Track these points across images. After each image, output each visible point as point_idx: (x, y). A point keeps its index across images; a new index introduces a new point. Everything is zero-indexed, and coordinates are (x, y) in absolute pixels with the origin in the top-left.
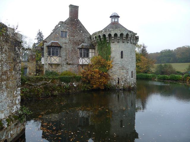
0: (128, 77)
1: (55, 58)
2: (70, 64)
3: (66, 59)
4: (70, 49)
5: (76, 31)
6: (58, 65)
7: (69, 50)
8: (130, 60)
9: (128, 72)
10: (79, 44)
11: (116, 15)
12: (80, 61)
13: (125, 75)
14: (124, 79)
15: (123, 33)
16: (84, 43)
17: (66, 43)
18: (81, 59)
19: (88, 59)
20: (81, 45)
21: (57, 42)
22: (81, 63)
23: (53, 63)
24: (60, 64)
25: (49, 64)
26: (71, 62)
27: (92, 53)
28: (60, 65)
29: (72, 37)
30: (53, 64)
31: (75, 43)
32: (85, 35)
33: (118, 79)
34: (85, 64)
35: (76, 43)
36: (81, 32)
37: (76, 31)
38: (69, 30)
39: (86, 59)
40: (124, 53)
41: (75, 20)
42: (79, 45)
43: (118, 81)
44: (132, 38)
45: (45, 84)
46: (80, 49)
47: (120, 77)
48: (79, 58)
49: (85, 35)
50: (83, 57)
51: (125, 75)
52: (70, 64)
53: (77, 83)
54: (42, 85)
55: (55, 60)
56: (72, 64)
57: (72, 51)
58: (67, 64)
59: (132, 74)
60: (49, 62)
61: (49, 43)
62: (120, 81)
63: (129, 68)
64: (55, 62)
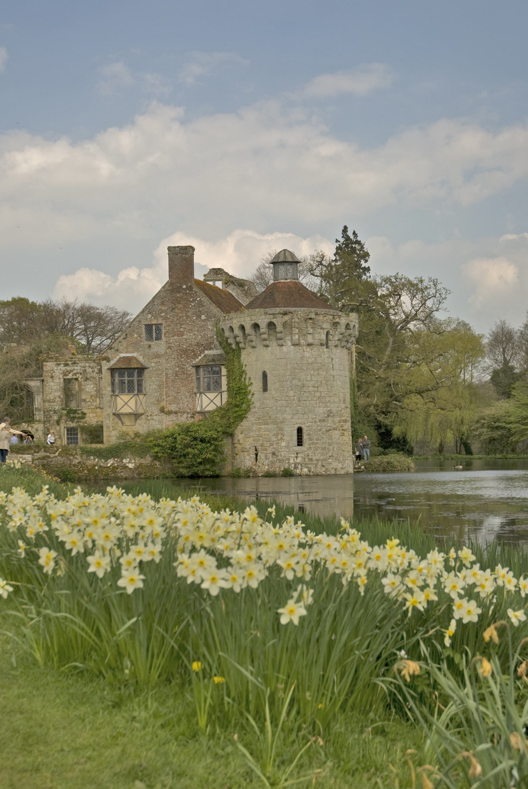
0: (283, 444)
1: (125, 397)
2: (169, 413)
3: (159, 401)
4: (170, 372)
5: (187, 317)
6: (136, 416)
7: (167, 374)
8: (291, 393)
9: (281, 429)
10: (196, 356)
13: (274, 439)
14: (270, 450)
15: (259, 322)
16: (211, 349)
17: (157, 356)
18: (198, 395)
19: (220, 395)
20: (203, 355)
21: (135, 355)
22: (199, 409)
23: (121, 411)
24: (142, 414)
25: (114, 414)
26: (173, 407)
28: (143, 417)
29: (176, 337)
30: (122, 414)
31: (185, 351)
35: (186, 353)
36: (203, 317)
37: (187, 317)
38: (165, 318)
39: (211, 395)
40: (269, 376)
41: (184, 287)
42: (196, 356)
45: (44, 458)
46: (197, 367)
47: (258, 445)
48: (195, 394)
50: (202, 390)
52: (169, 413)
53: (135, 460)
54: (37, 459)
55: (126, 404)
56: (176, 413)
57: (176, 375)
58: (162, 410)
60: (114, 412)
61: (115, 360)
62: (259, 454)
64: (126, 410)
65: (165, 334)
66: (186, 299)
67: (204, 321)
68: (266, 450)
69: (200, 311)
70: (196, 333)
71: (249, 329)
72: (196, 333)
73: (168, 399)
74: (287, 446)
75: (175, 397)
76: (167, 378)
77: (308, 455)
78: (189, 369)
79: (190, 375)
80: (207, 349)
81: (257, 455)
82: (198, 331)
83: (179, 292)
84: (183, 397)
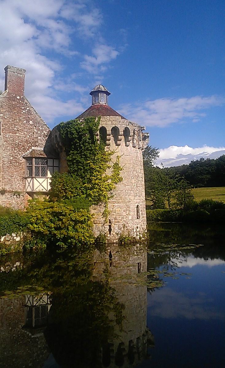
5: (20, 120)
8: (133, 181)
11: (103, 90)
12: (27, 184)
13: (124, 214)
14: (122, 223)
15: (118, 126)
16: (36, 146)
18: (29, 180)
20: (30, 150)
22: (29, 190)
27: (53, 166)
29: (11, 134)
32: (39, 130)
33: (110, 223)
34: (37, 190)
36: (31, 122)
37: (20, 120)
39: (41, 180)
41: (18, 98)
43: (110, 226)
44: (136, 137)
49: (39, 130)
50: (34, 176)
51: (124, 214)
59: (138, 212)
62: (113, 225)
63: (132, 198)
65: (3, 130)
66: (20, 107)
67: (31, 125)
68: (118, 222)
69: (29, 117)
70: (25, 133)
71: (109, 131)
72: (25, 133)
73: (4, 181)
74: (132, 220)
75: (9, 180)
76: (4, 164)
77: (142, 226)
78: (21, 159)
79: (21, 163)
80: (33, 146)
81: (110, 226)
82: (27, 131)
83: (14, 101)
84: (16, 180)
